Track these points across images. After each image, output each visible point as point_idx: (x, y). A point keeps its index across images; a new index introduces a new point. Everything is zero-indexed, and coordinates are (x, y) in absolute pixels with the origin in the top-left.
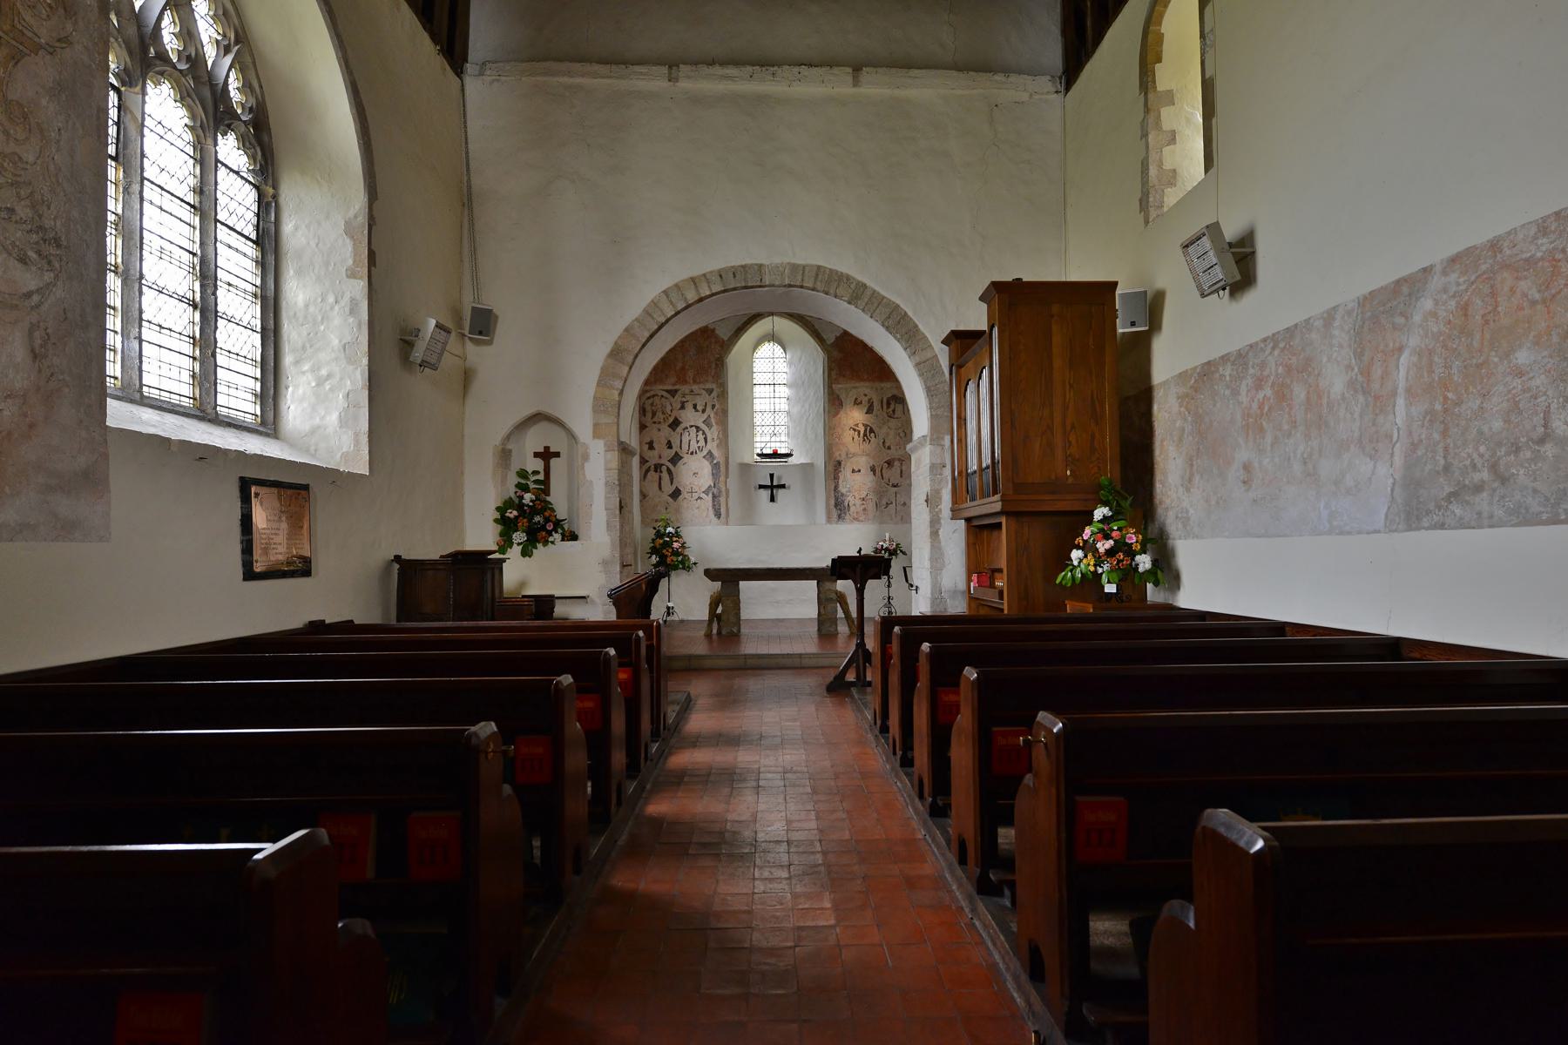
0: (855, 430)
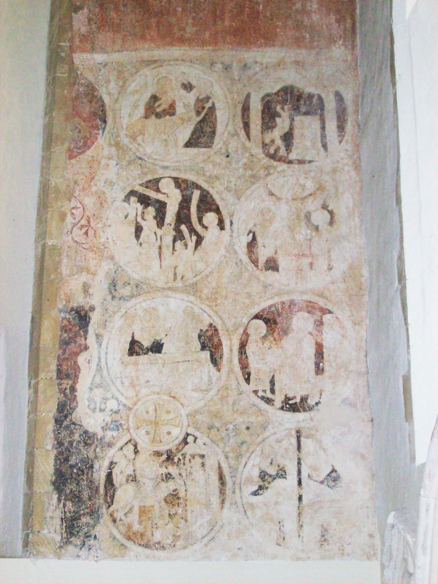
0: (144, 201)
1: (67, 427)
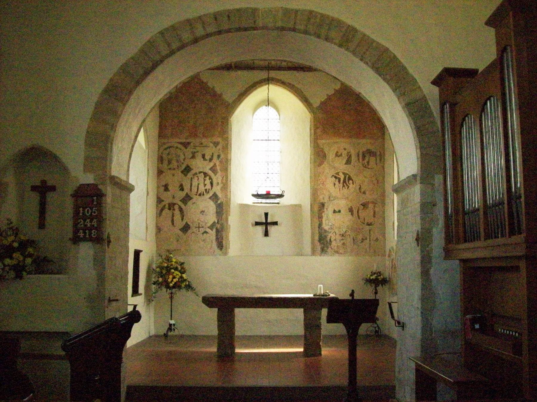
1: (321, 229)
